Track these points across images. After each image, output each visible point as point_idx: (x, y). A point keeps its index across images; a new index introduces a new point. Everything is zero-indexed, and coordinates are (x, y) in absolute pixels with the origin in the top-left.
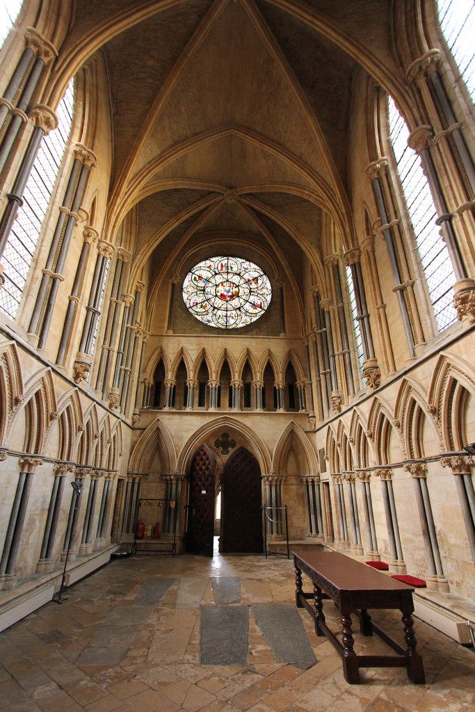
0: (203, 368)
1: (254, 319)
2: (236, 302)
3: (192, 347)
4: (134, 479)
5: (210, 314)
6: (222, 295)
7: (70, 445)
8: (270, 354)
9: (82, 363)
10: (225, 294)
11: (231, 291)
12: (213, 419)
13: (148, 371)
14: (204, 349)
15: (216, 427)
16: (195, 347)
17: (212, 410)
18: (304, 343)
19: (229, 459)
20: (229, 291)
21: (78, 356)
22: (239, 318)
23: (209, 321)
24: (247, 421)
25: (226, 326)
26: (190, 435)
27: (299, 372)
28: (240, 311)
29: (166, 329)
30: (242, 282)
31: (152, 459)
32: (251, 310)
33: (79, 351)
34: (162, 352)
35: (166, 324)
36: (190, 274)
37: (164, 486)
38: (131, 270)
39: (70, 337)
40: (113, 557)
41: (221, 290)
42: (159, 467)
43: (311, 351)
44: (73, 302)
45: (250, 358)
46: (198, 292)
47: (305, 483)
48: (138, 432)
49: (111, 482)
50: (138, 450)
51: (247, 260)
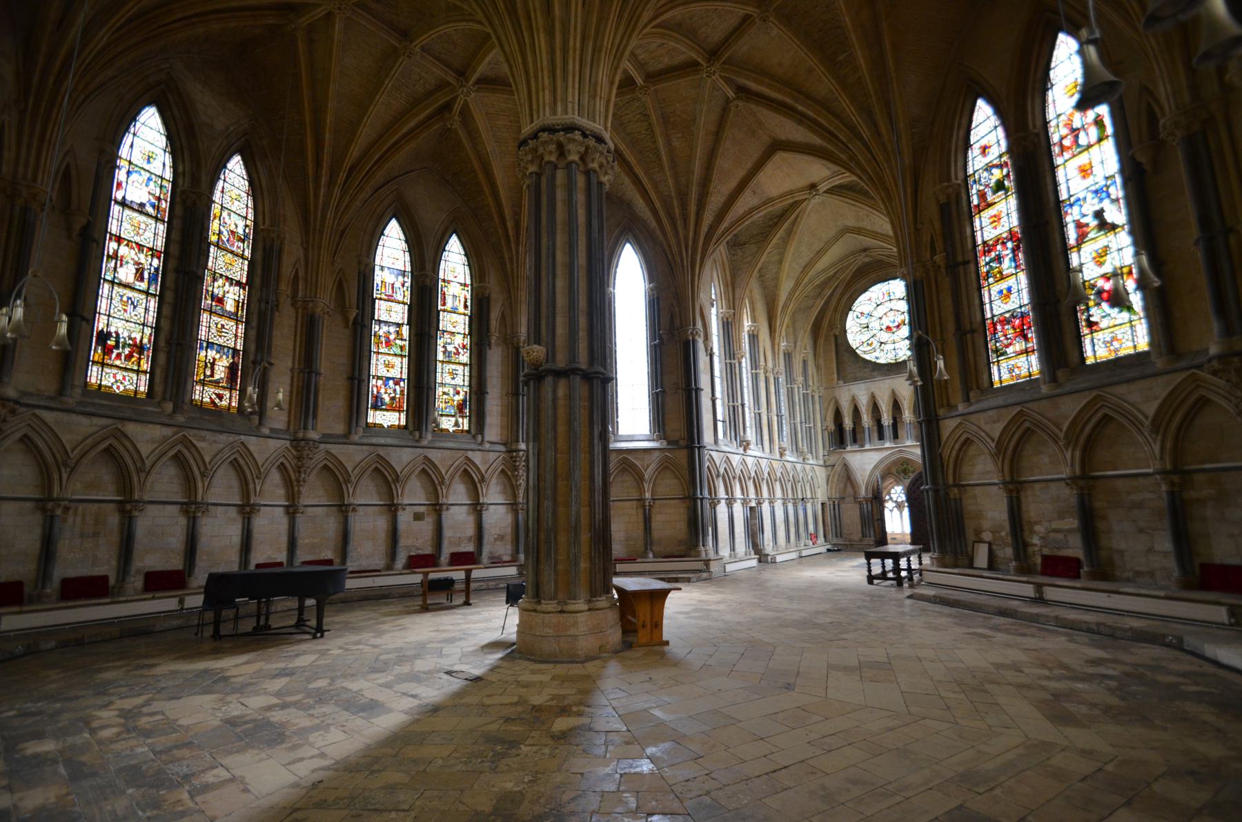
0: (875, 409)
3: (861, 392)
4: (834, 502)
5: (878, 351)
10: (891, 325)
12: (889, 452)
13: (828, 419)
14: (872, 393)
15: (893, 458)
16: (864, 392)
17: (888, 445)
19: (911, 482)
23: (877, 358)
26: (872, 466)
29: (836, 380)
31: (845, 487)
34: (837, 402)
35: (835, 376)
36: (851, 313)
37: (858, 506)
41: (886, 322)
42: (852, 492)
48: (830, 468)
50: (832, 481)
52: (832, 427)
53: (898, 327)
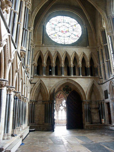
1: (75, 41)
2: (68, 34)
4: (32, 103)
5: (58, 38)
6: (62, 31)
7: (19, 85)
8: (84, 54)
9: (23, 51)
10: (63, 30)
11: (66, 29)
18: (97, 50)
20: (65, 30)
21: (21, 48)
22: (70, 40)
24: (77, 80)
25: (64, 43)
27: (95, 61)
28: (70, 37)
30: (70, 26)
32: (74, 37)
33: (21, 46)
37: (44, 105)
38: (31, 18)
39: (19, 39)
40: (30, 131)
41: (61, 29)
43: (100, 53)
44: (19, 25)
45: (76, 56)
46: (52, 30)
47: (98, 104)
48: (33, 85)
49: (26, 103)
51: (71, 17)
52: (36, 64)
53: (66, 31)
